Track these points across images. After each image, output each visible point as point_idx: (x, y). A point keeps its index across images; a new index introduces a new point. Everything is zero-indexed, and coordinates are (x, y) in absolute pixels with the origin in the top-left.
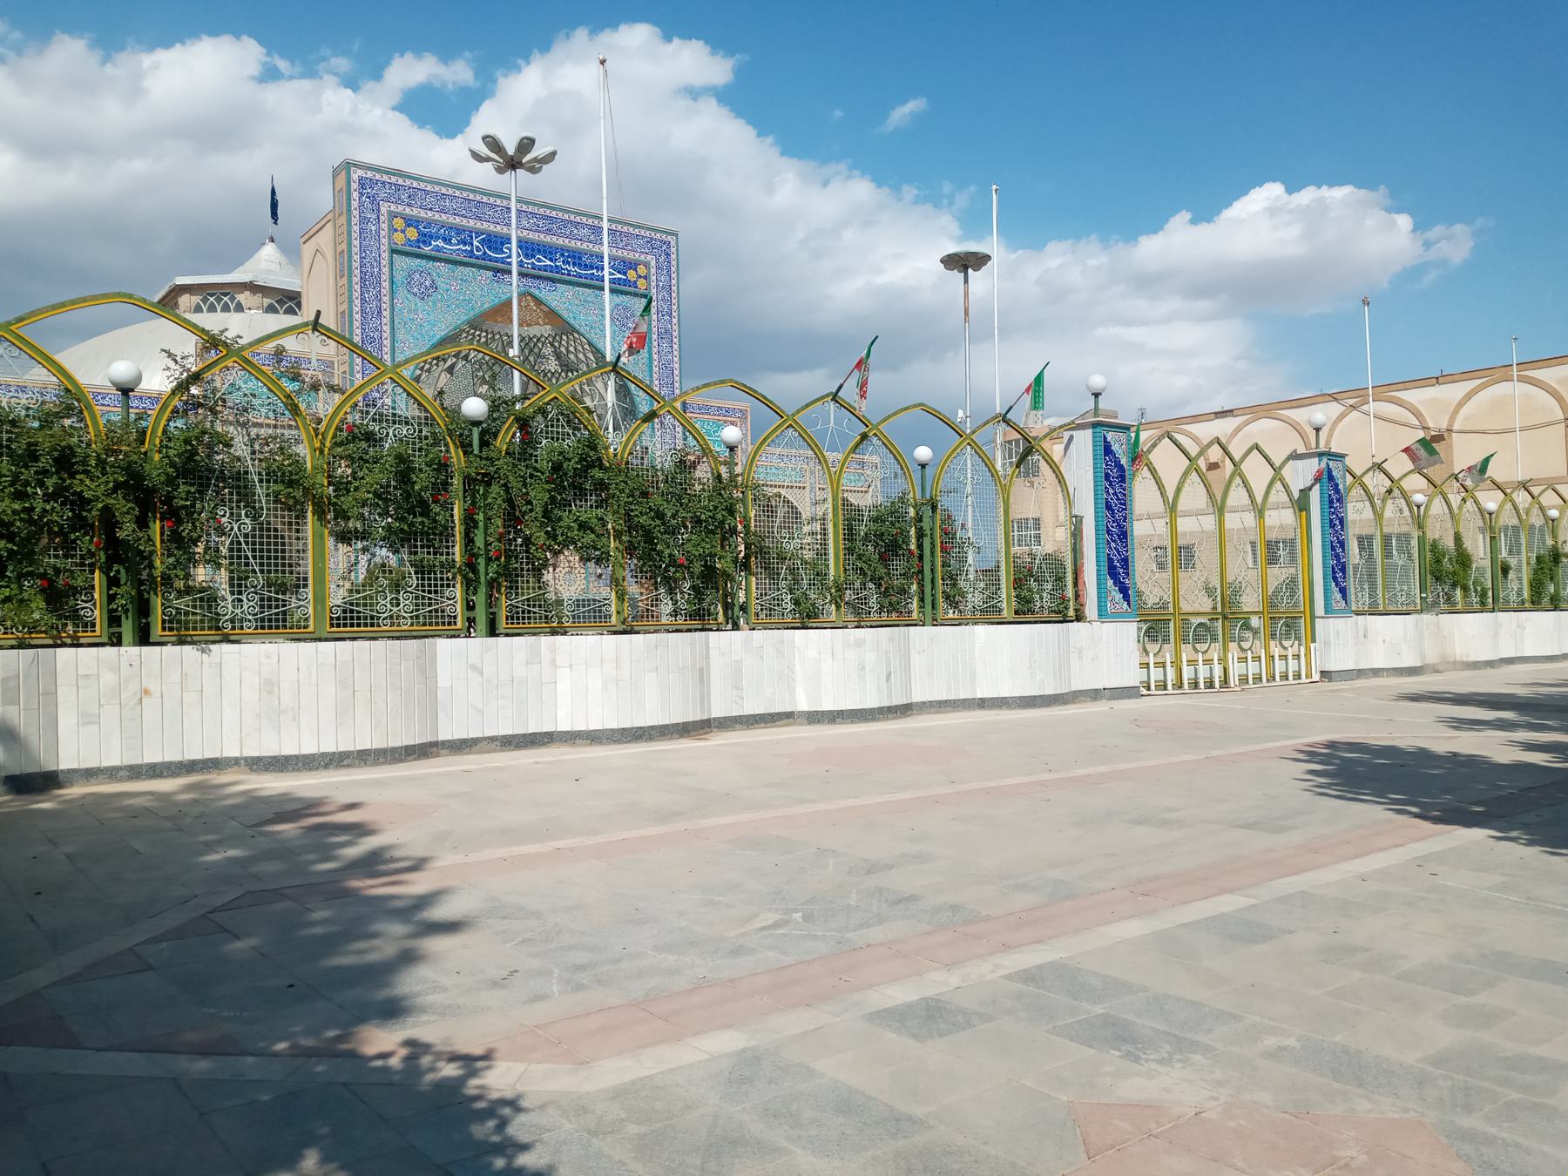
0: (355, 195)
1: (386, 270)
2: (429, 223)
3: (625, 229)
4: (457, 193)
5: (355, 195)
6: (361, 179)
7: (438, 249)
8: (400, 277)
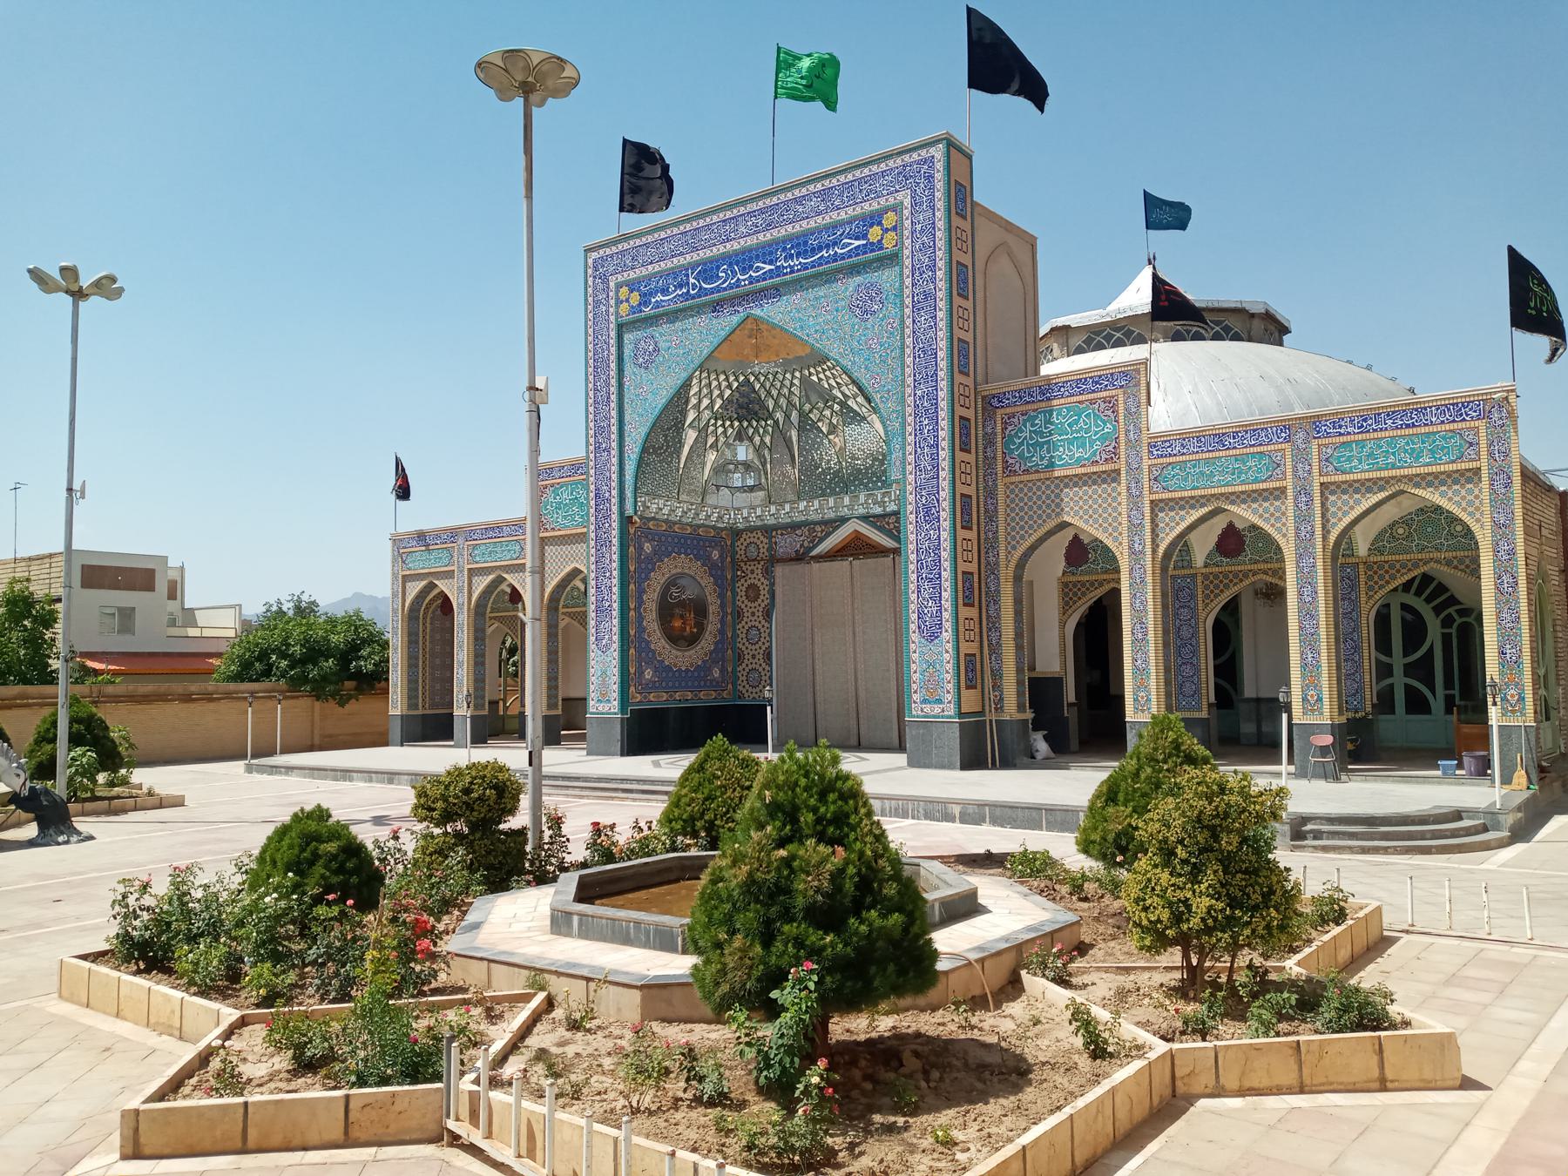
0: (590, 280)
1: (613, 350)
2: (649, 277)
3: (866, 171)
4: (676, 231)
5: (590, 280)
6: (595, 261)
7: (658, 305)
8: (627, 352)
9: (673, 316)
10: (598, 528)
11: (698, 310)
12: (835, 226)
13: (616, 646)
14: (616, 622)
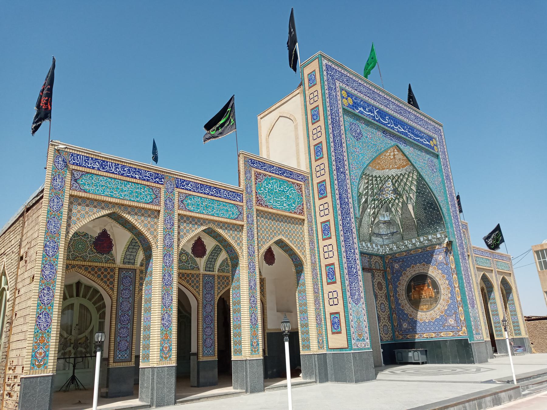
9: (368, 123)
10: (343, 219)
11: (378, 128)
12: (421, 132)
13: (363, 300)
14: (361, 283)
